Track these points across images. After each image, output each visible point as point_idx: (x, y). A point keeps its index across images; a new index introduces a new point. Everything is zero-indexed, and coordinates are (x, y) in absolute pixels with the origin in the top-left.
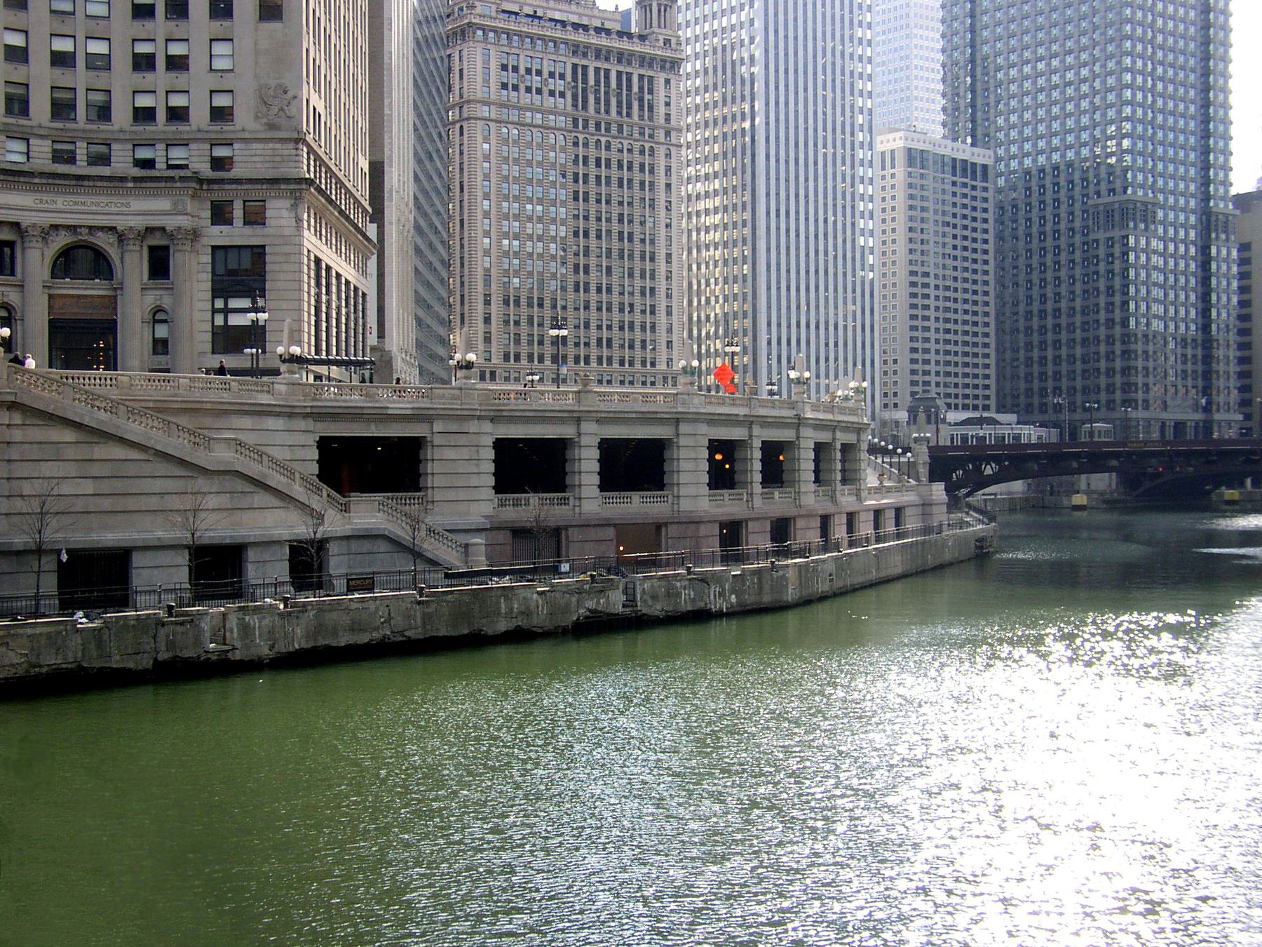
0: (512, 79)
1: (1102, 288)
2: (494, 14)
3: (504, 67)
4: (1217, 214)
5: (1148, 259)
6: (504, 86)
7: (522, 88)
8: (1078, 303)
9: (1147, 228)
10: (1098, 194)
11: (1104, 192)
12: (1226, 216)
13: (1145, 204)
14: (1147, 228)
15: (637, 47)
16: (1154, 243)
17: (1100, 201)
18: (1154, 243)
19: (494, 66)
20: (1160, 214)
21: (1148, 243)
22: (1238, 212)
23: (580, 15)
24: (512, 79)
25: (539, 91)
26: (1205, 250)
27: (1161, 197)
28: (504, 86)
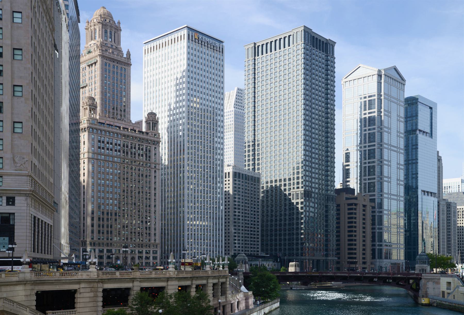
0: (102, 145)
1: (295, 218)
2: (96, 123)
3: (99, 141)
4: (330, 195)
5: (309, 209)
6: (99, 148)
7: (106, 149)
8: (287, 222)
9: (309, 199)
10: (294, 188)
11: (295, 188)
12: (333, 196)
13: (308, 192)
14: (309, 199)
15: (145, 136)
16: (311, 204)
17: (294, 190)
18: (311, 204)
19: (96, 141)
20: (313, 195)
21: (309, 204)
22: (336, 195)
23: (126, 125)
24: (102, 145)
25: (111, 150)
26: (327, 206)
27: (313, 190)
28: (99, 148)
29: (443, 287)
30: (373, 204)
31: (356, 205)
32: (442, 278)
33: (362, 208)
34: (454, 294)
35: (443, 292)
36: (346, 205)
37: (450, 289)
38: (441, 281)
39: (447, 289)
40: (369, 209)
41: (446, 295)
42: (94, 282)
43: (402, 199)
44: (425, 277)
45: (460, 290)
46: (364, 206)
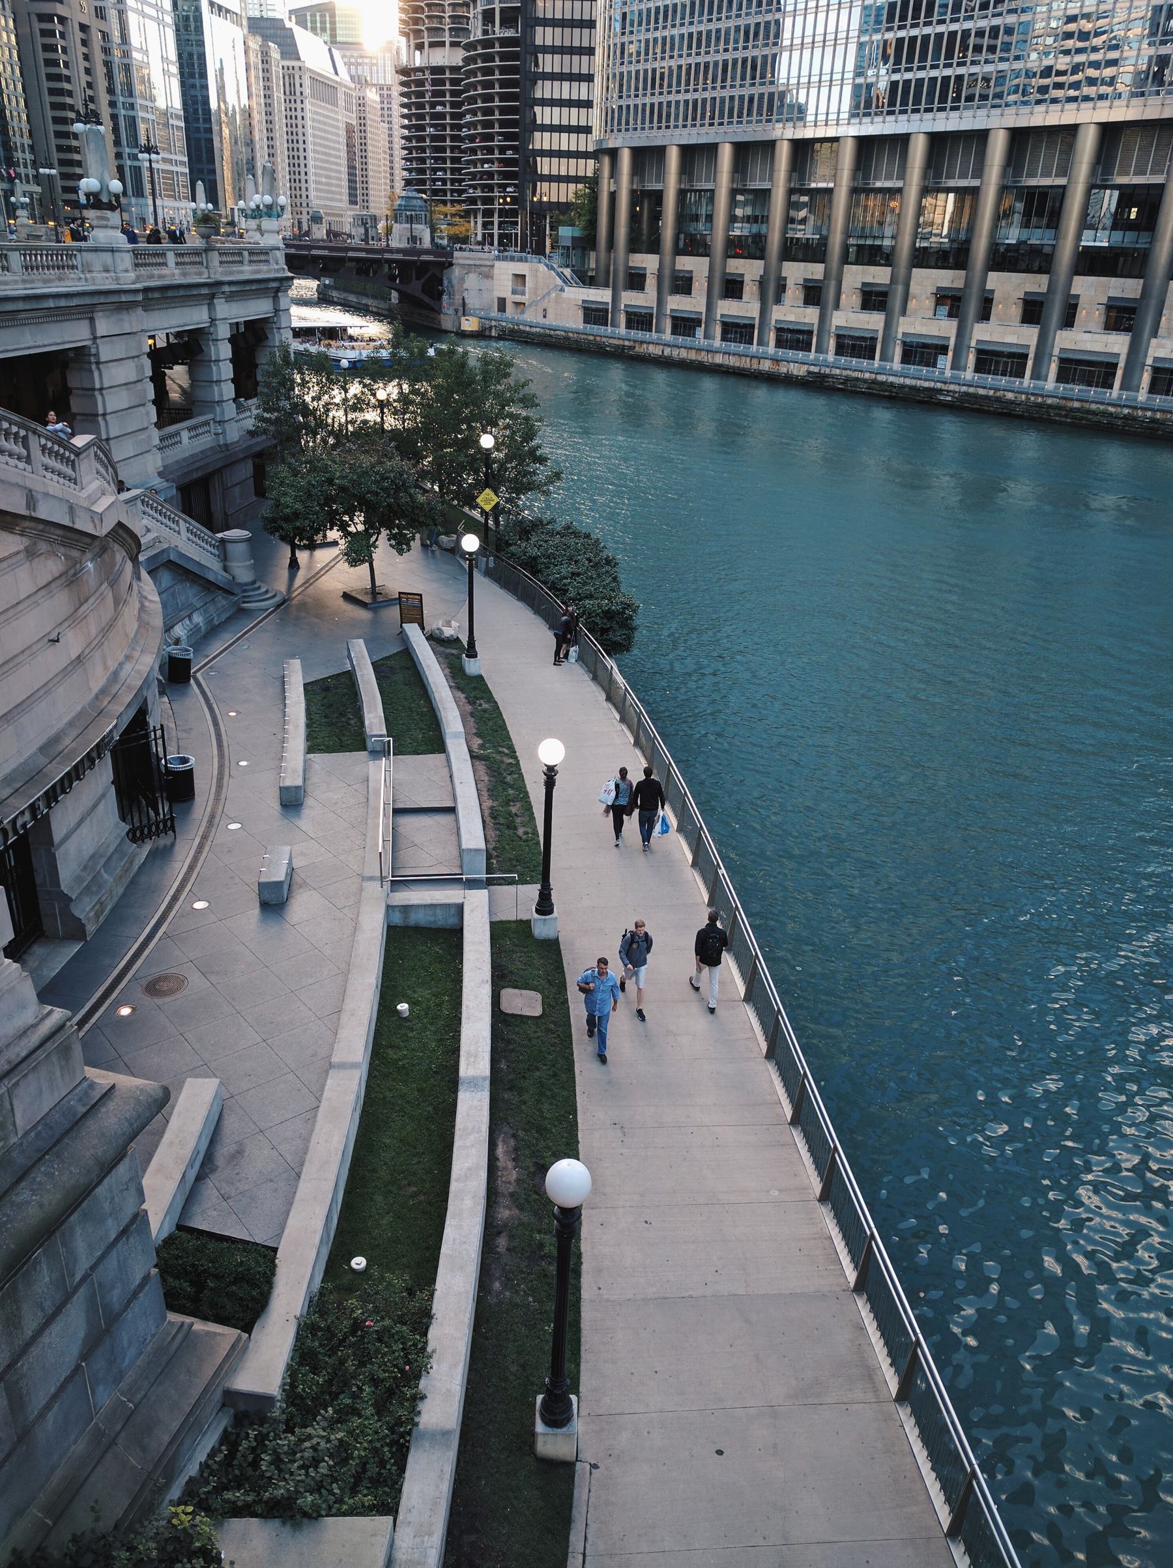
29: (502, 284)
30: (101, 25)
31: (62, 20)
32: (497, 264)
33: (79, 35)
34: (544, 304)
35: (502, 303)
36: (34, 19)
37: (523, 293)
38: (496, 271)
39: (514, 292)
40: (96, 38)
41: (509, 307)
42: (129, 306)
43: (169, 19)
44: (461, 262)
45: (564, 295)
46: (84, 28)
